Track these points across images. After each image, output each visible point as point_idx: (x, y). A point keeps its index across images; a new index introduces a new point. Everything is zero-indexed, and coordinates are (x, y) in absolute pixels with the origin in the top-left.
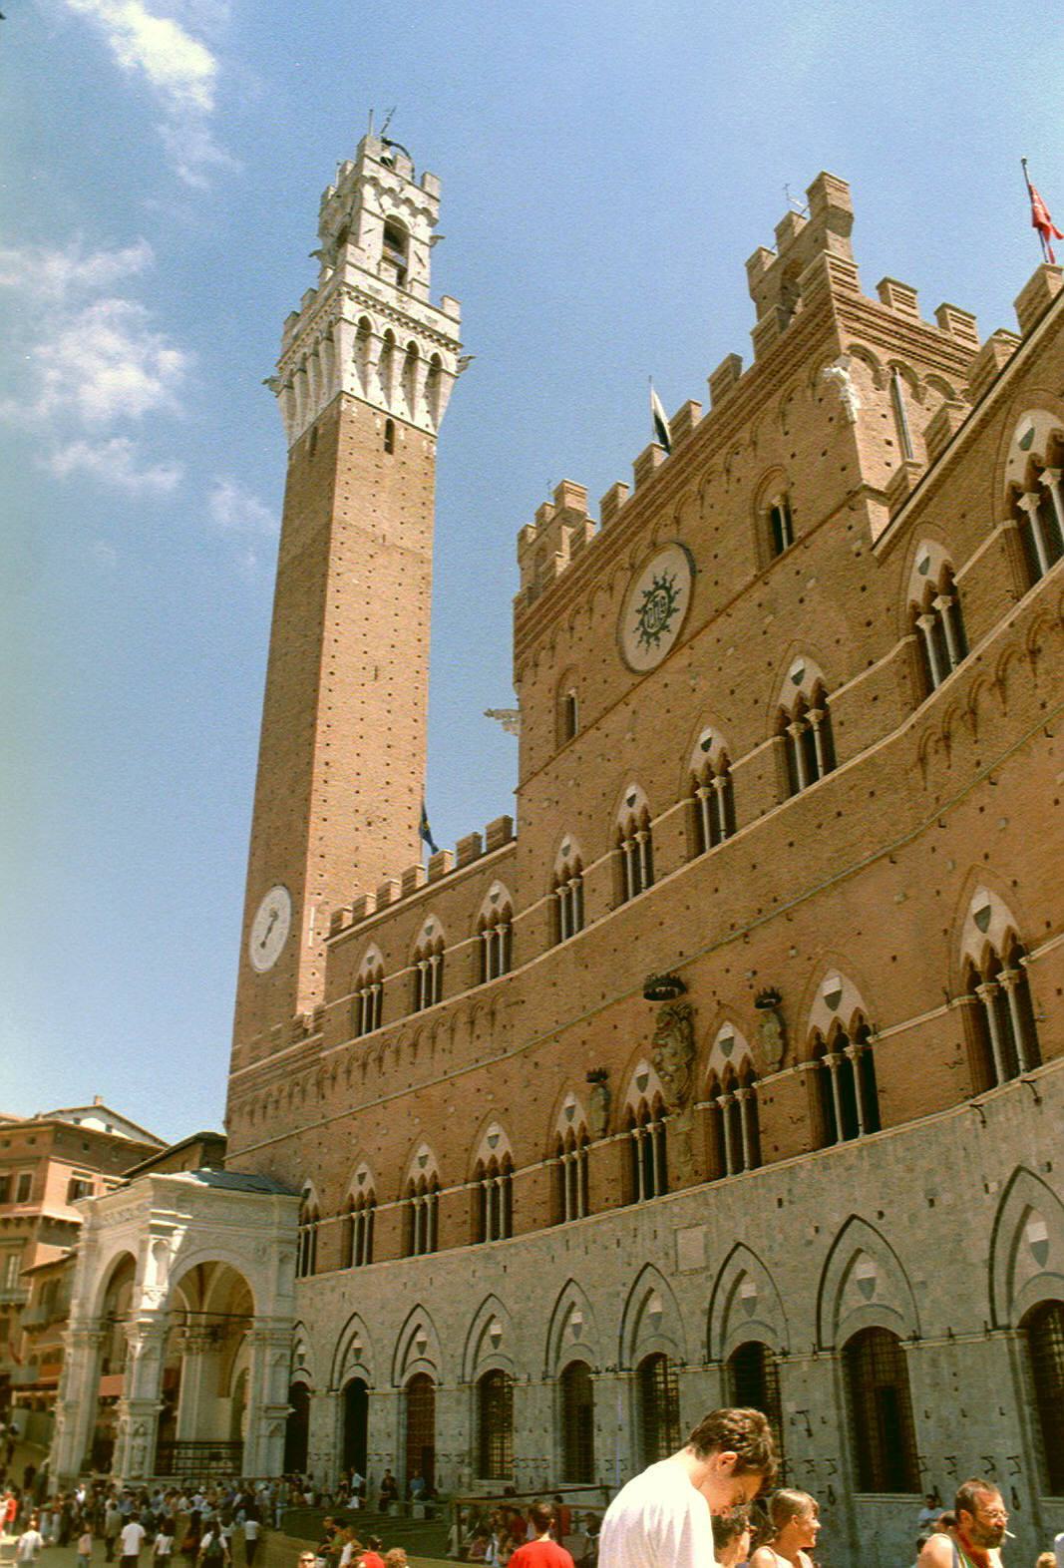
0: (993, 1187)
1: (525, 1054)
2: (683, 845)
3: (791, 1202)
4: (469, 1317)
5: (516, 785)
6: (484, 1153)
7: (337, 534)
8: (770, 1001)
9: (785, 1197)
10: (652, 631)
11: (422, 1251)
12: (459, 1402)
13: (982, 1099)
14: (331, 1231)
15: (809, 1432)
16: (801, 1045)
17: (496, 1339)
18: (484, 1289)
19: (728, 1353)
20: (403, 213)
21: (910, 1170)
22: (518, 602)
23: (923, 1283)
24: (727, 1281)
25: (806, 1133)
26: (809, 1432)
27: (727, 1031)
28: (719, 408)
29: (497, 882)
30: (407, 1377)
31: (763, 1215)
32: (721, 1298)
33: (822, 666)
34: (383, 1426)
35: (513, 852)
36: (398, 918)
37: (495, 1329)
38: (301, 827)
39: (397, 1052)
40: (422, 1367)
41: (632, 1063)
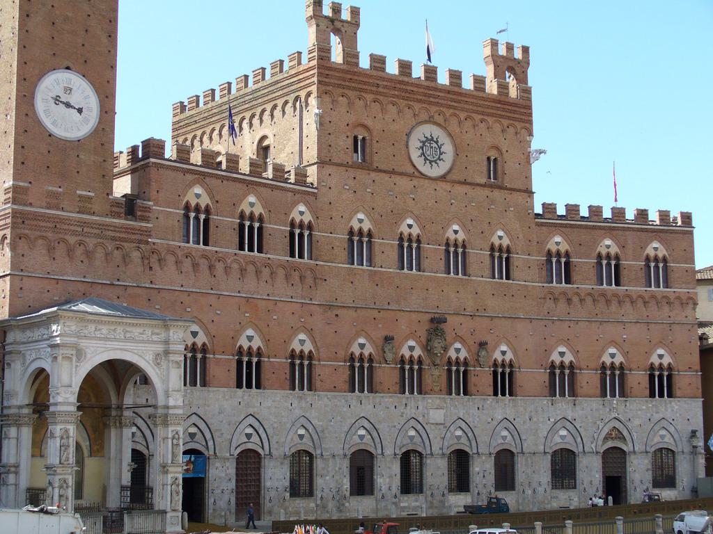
0: (552, 420)
1: (330, 307)
2: (442, 264)
3: (483, 409)
4: (288, 426)
6: (296, 346)
8: (482, 345)
9: (481, 407)
10: (429, 158)
11: (249, 386)
12: (282, 463)
13: (554, 398)
15: (484, 476)
16: (491, 363)
17: (301, 437)
18: (298, 412)
21: (525, 410)
23: (525, 440)
26: (484, 476)
27: (458, 345)
28: (475, 93)
29: (301, 204)
30: (239, 450)
31: (471, 411)
32: (449, 434)
33: (510, 240)
34: (223, 475)
36: (225, 182)
37: (302, 432)
38: (104, 39)
40: (250, 446)
41: (407, 339)
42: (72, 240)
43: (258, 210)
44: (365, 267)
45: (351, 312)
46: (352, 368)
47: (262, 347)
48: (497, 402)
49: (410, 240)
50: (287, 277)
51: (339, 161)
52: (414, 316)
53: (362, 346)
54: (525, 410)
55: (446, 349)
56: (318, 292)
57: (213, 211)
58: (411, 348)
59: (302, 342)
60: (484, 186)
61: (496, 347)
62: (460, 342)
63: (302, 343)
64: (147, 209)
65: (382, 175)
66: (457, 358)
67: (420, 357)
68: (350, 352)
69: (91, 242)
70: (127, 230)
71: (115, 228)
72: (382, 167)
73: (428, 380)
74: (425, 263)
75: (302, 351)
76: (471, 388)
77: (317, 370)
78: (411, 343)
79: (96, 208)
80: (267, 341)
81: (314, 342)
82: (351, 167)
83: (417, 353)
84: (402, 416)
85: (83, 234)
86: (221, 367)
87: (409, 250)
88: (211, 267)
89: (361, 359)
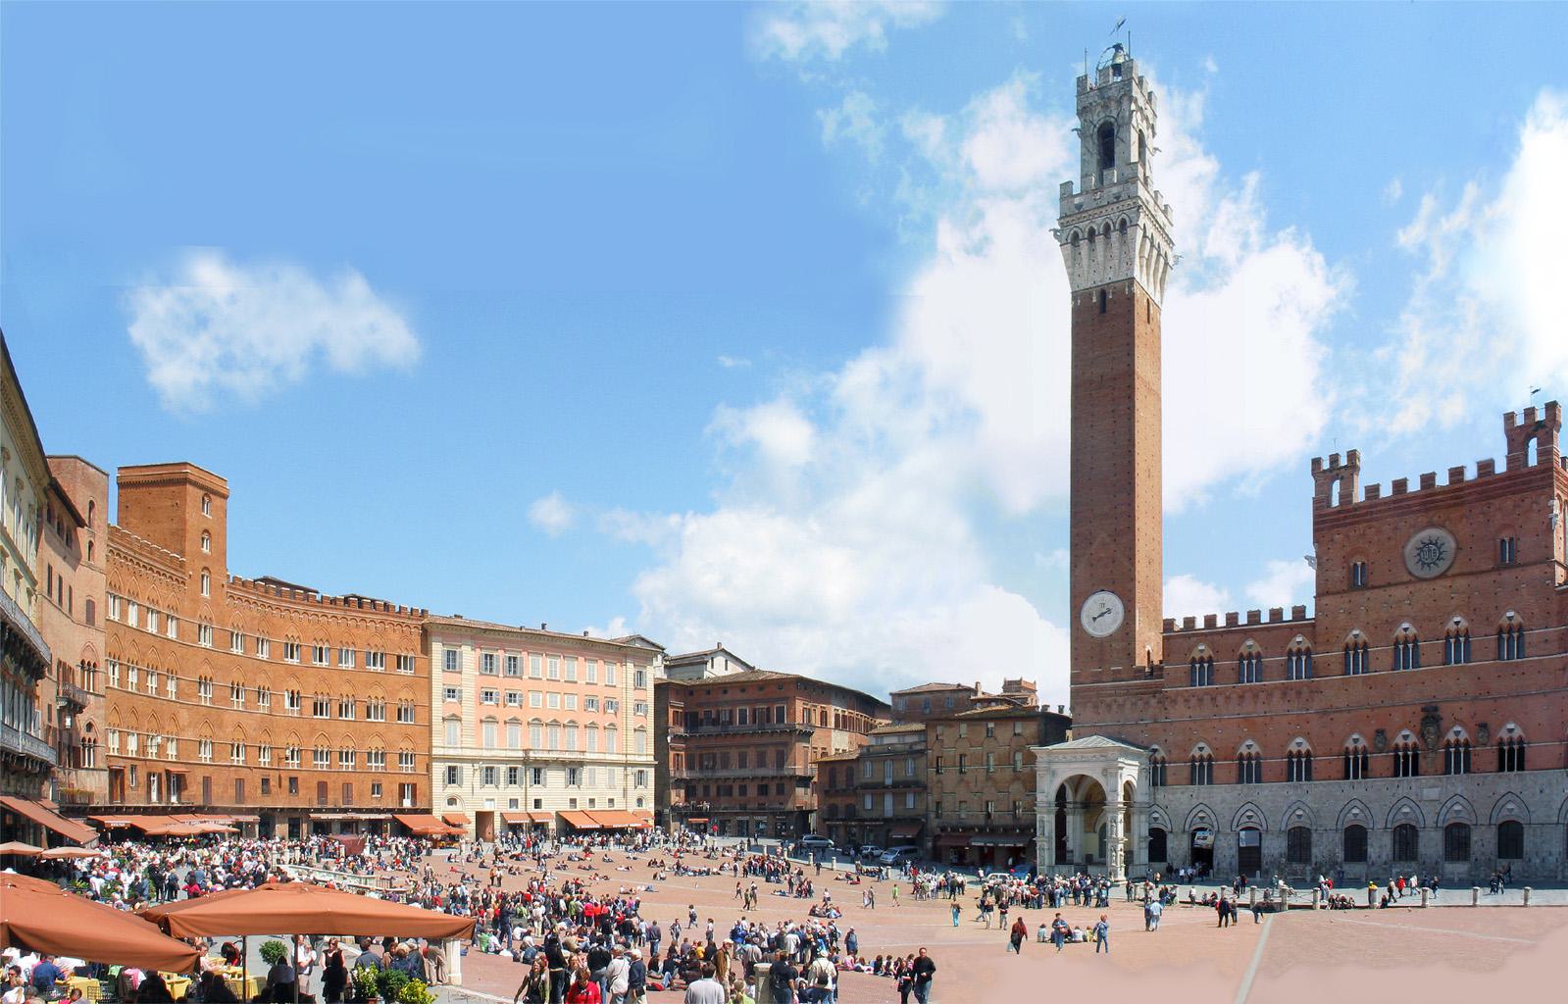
1: (1324, 713)
5: (1315, 594)
6: (1293, 748)
7: (1138, 383)
14: (1177, 769)
15: (1483, 845)
16: (1494, 743)
19: (1446, 825)
20: (1143, 126)
21: (1535, 783)
22: (1316, 501)
23: (1534, 812)
24: (1449, 804)
25: (1495, 764)
26: (1483, 845)
27: (1458, 728)
32: (1445, 810)
35: (1313, 625)
36: (1225, 636)
39: (1228, 698)
41: (1401, 729)
42: (1108, 700)
43: (1256, 649)
44: (1361, 675)
45: (1345, 715)
46: (1347, 760)
47: (1261, 753)
48: (1500, 777)
49: (1406, 642)
50: (1284, 694)
51: (1334, 590)
52: (1408, 708)
53: (1356, 741)
54: (1535, 783)
55: (1440, 735)
56: (1315, 703)
57: (1215, 659)
58: (1405, 737)
59: (1299, 744)
60: (1489, 571)
61: (1501, 725)
62: (1460, 725)
63: (1299, 744)
64: (1162, 669)
65: (1376, 591)
66: (1457, 741)
67: (1415, 744)
68: (1344, 748)
69: (1120, 700)
70: (1147, 686)
71: (1136, 685)
72: (1376, 584)
73: (1422, 762)
74: (1422, 660)
75: (1299, 752)
76: (1472, 767)
77: (1314, 765)
78: (1406, 732)
79: (1123, 676)
80: (1264, 746)
81: (1311, 743)
82: (1344, 592)
83: (1412, 740)
84: (1394, 796)
85: (1116, 695)
86: (1224, 768)
87: (1406, 652)
88: (1213, 699)
89: (1356, 750)
